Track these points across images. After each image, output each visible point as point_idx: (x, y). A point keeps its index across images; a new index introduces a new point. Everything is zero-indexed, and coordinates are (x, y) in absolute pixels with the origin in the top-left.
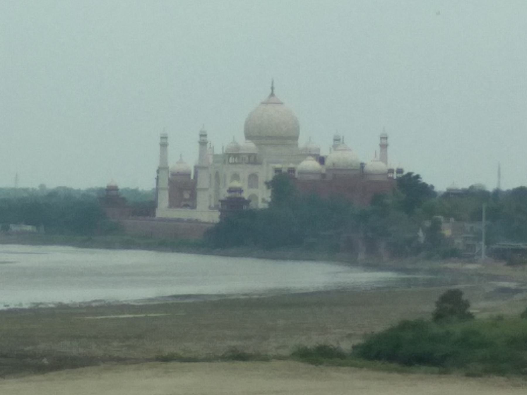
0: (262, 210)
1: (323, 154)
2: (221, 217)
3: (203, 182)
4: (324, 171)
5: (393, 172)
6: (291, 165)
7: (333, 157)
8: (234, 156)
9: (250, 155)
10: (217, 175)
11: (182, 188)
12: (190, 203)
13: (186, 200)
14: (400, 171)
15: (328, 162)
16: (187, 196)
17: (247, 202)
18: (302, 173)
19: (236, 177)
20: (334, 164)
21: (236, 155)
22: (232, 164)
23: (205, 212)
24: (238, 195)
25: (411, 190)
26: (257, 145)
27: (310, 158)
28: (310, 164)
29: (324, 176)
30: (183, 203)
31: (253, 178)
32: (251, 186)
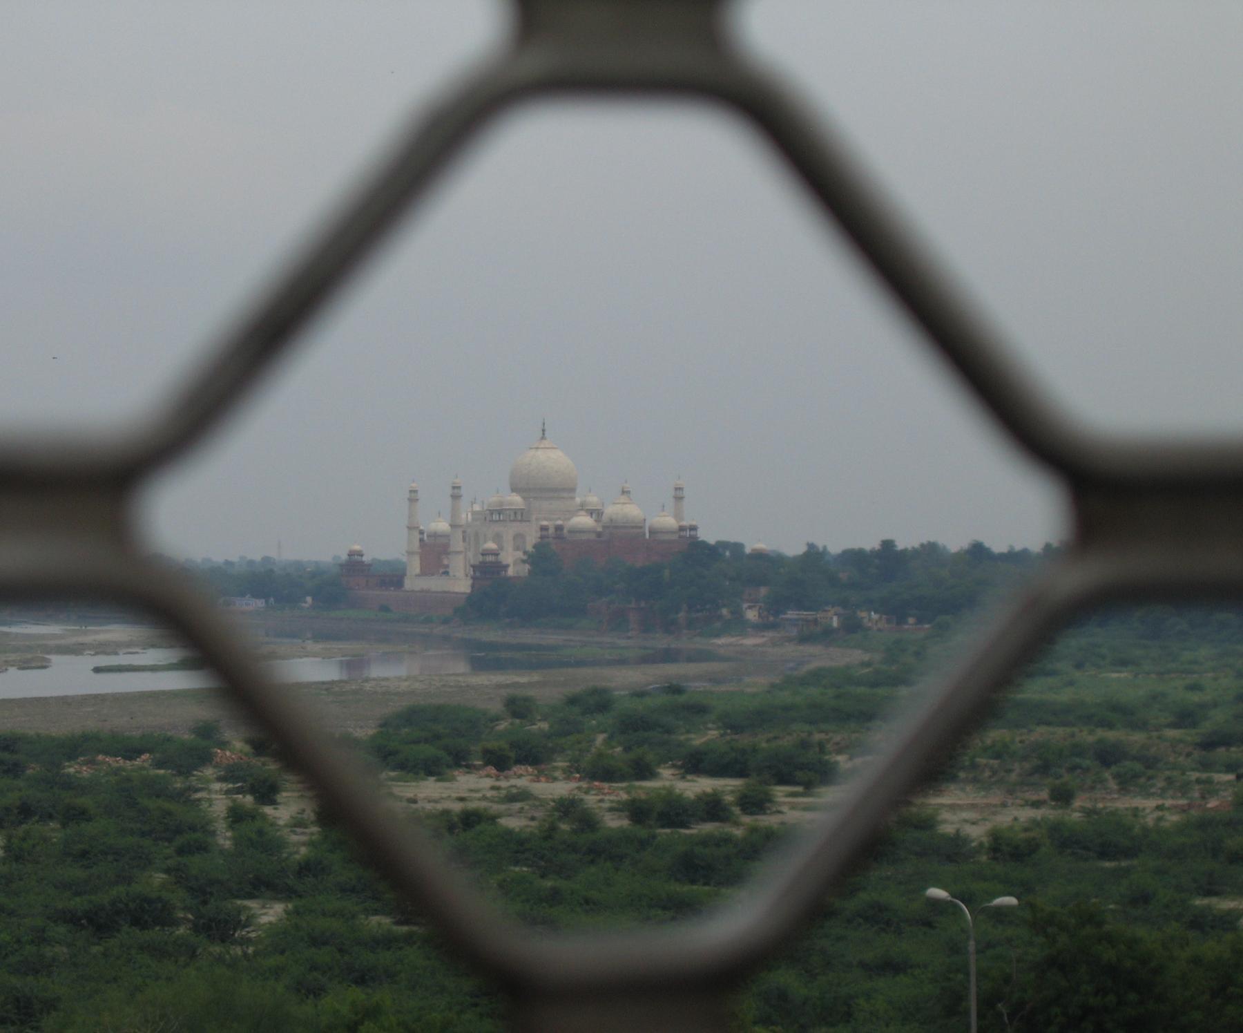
3: (457, 544)
7: (611, 511)
8: (496, 514)
10: (477, 535)
11: (434, 552)
14: (693, 528)
15: (605, 518)
21: (500, 512)
23: (460, 583)
26: (524, 498)
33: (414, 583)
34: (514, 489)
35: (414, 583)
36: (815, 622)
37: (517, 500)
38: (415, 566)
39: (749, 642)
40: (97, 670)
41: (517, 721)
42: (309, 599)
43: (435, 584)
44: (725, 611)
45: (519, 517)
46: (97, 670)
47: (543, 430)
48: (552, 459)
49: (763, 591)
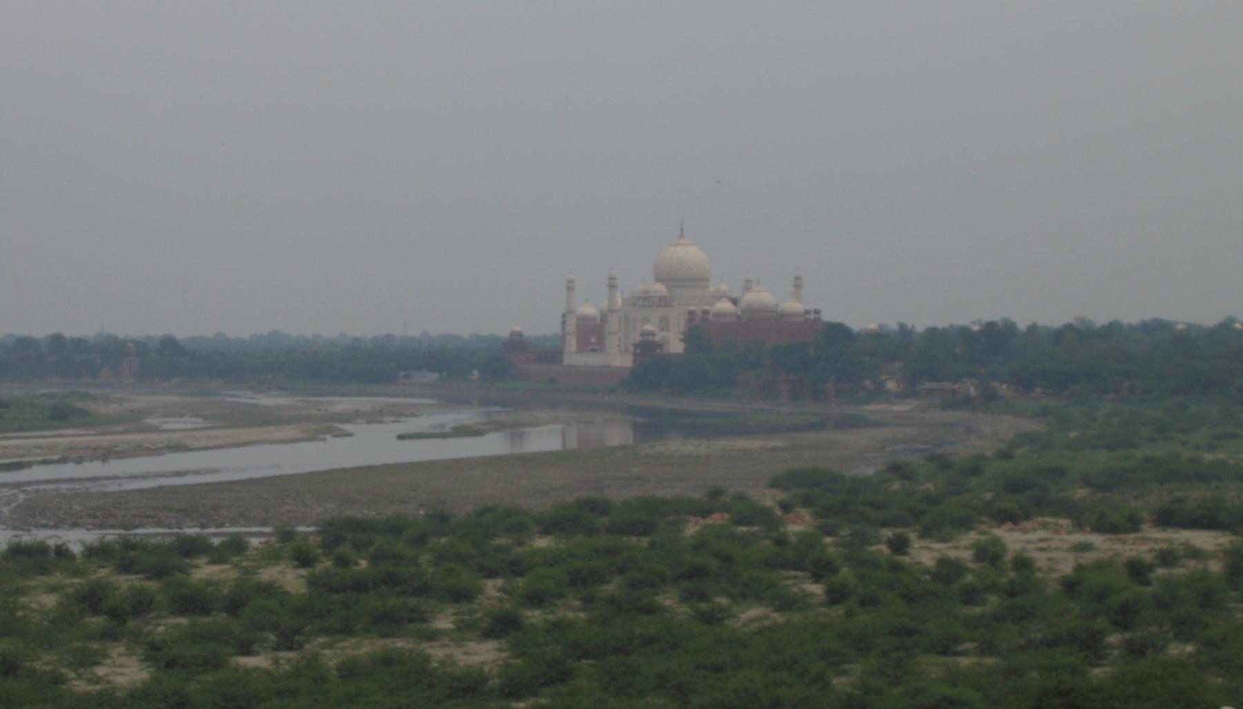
0: (678, 355)
1: (734, 295)
2: (634, 361)
3: (613, 324)
6: (706, 307)
7: (751, 297)
8: (645, 301)
9: (660, 298)
11: (591, 333)
14: (817, 312)
15: (743, 303)
16: (593, 340)
17: (660, 345)
18: (717, 315)
19: (646, 320)
21: (645, 299)
23: (618, 358)
24: (651, 338)
25: (838, 332)
28: (725, 306)
29: (738, 317)
31: (664, 323)
32: (662, 329)
33: (573, 358)
34: (658, 279)
35: (573, 358)
36: (953, 391)
37: (661, 288)
38: (572, 344)
39: (899, 408)
40: (401, 437)
41: (906, 483)
42: (476, 372)
43: (592, 360)
44: (867, 382)
46: (401, 437)
48: (690, 254)
49: (897, 365)
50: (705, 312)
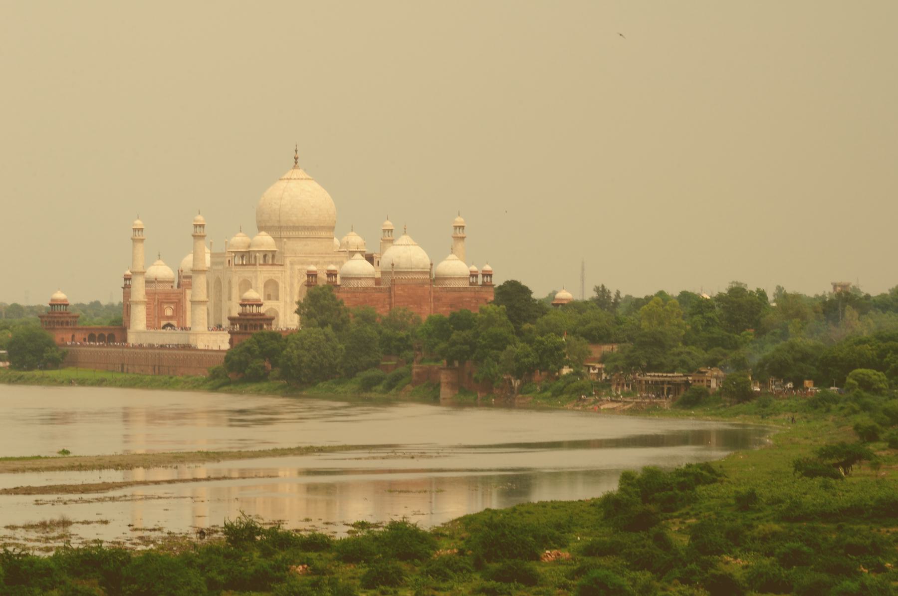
2: (231, 342)
4: (378, 275)
5: (477, 276)
6: (332, 267)
10: (218, 282)
11: (168, 300)
12: (174, 323)
13: (168, 318)
16: (169, 312)
17: (270, 320)
20: (393, 265)
22: (239, 265)
27: (358, 256)
29: (378, 281)
30: (164, 323)
32: (269, 297)
45: (270, 262)
47: (296, 158)
50: (331, 274)
